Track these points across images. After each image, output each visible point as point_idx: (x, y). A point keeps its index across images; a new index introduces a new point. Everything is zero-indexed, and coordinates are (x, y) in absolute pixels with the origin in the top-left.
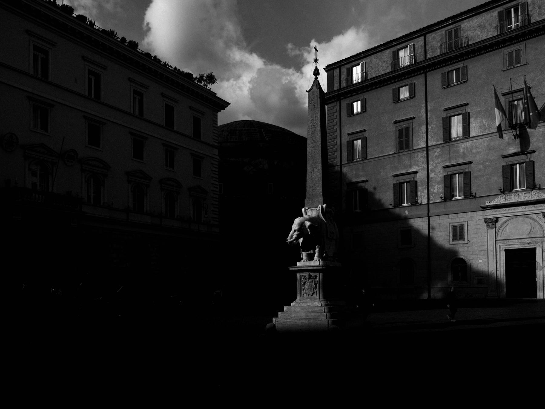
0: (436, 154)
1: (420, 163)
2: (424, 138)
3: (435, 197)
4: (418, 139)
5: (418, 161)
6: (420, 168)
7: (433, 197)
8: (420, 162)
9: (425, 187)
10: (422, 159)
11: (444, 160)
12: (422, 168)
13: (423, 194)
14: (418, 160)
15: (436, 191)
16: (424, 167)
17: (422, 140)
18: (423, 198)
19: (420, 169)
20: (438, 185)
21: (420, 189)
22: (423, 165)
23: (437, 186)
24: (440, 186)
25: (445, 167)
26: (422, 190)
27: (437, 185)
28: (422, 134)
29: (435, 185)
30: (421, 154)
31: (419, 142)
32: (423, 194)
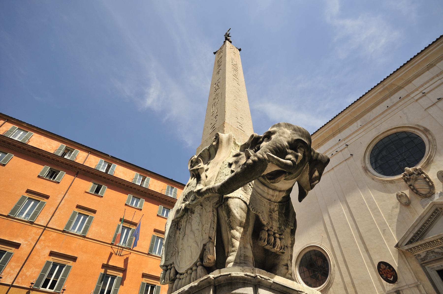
0: (50, 237)
2: (48, 218)
3: (23, 280)
5: (28, 235)
6: (27, 242)
7: (22, 279)
8: (31, 237)
9: (19, 264)
10: (34, 235)
11: (55, 245)
13: (12, 272)
14: (29, 234)
15: (28, 274)
16: (31, 244)
17: (45, 218)
18: (9, 276)
19: (25, 244)
20: (34, 268)
21: (12, 265)
24: (37, 270)
25: (52, 254)
26: (13, 267)
27: (33, 268)
28: (48, 214)
29: (32, 267)
30: (36, 230)
32: (12, 272)
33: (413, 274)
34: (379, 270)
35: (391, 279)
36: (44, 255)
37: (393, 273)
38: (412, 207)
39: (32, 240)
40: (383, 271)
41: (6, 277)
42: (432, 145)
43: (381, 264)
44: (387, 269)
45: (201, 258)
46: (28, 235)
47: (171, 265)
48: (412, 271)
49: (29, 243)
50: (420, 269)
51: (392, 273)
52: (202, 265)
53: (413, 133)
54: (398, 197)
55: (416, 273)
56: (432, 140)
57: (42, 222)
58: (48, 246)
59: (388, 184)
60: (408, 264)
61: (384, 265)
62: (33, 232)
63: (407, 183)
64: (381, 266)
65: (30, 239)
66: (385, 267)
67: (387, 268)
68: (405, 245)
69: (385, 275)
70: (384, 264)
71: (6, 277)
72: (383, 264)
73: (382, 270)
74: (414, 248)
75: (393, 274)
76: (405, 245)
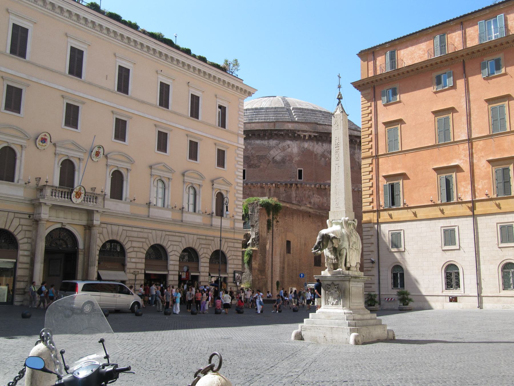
0: (479, 147)
1: (462, 157)
4: (459, 130)
5: (460, 154)
6: (462, 161)
8: (462, 155)
10: (463, 152)
12: (464, 161)
13: (466, 190)
14: (460, 153)
16: (466, 160)
18: (466, 194)
19: (462, 163)
21: (463, 184)
22: (465, 159)
23: (482, 182)
26: (465, 185)
29: (479, 181)
31: (460, 133)
32: (466, 190)
36: (484, 166)
39: (465, 156)
41: (465, 195)
46: (460, 154)
49: (464, 161)
57: (463, 136)
58: (483, 157)
62: (461, 150)
65: (462, 157)
71: (465, 195)
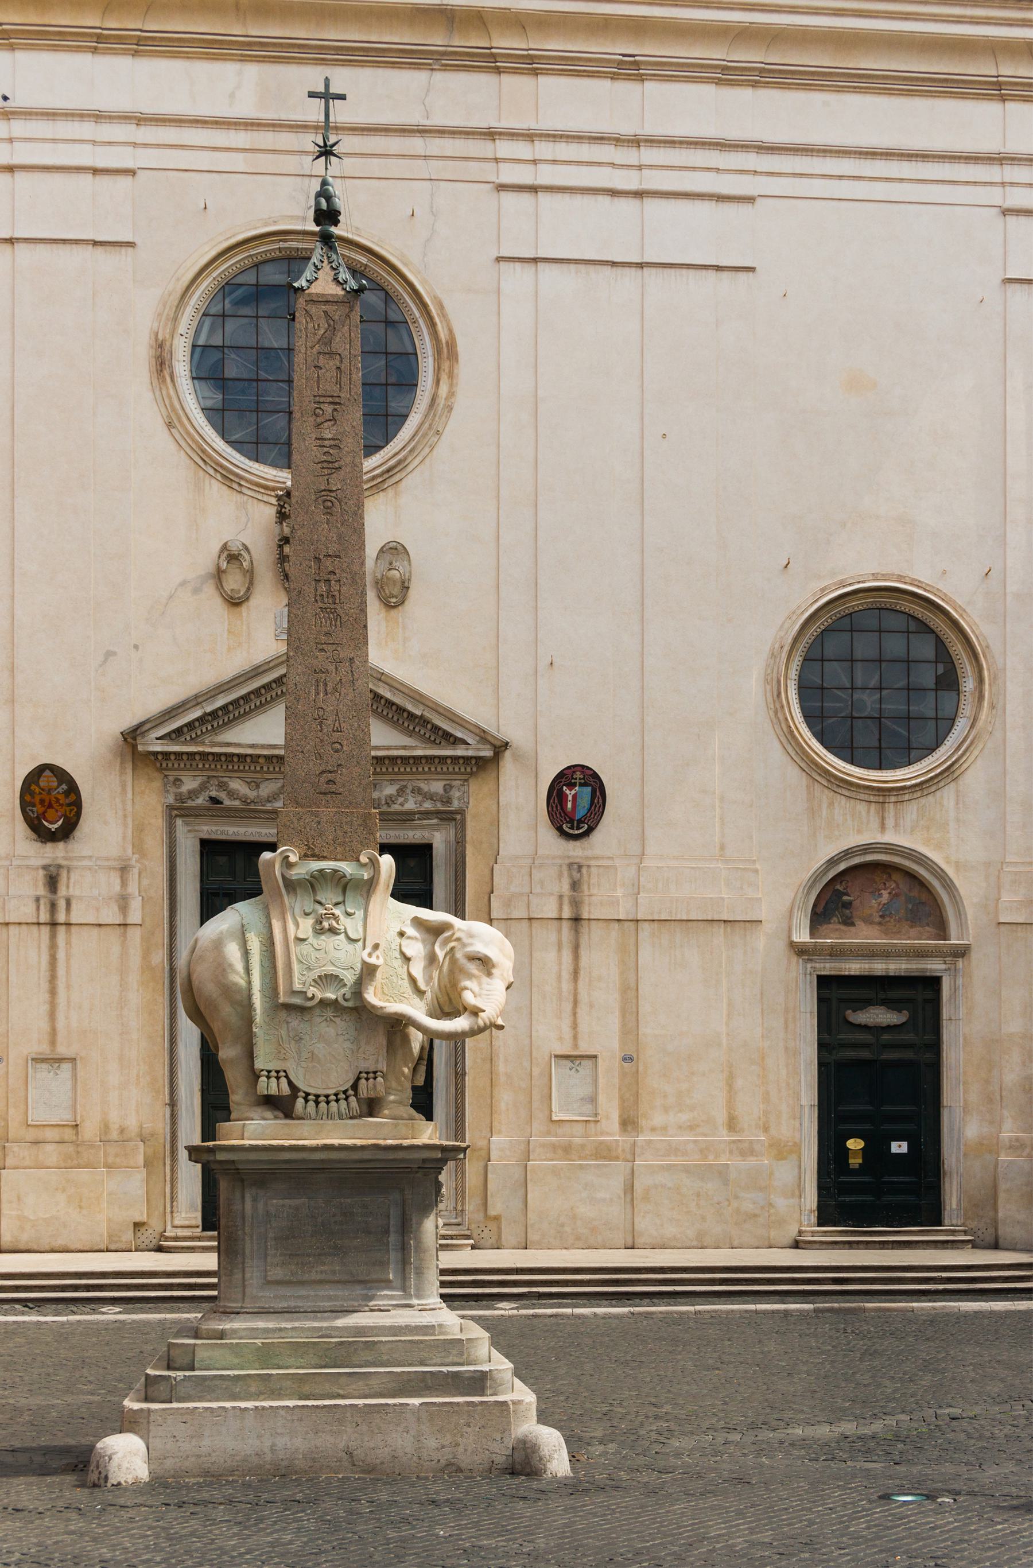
33: (130, 831)
34: (30, 786)
35: (50, 826)
37: (71, 811)
38: (244, 614)
40: (40, 793)
42: (430, 427)
43: (47, 773)
44: (58, 792)
45: (355, 1087)
47: (278, 1072)
48: (130, 821)
50: (158, 822)
51: (68, 809)
52: (356, 1095)
53: (407, 322)
54: (223, 557)
55: (139, 829)
56: (443, 402)
59: (213, 481)
60: (130, 795)
61: (55, 779)
63: (281, 523)
64: (41, 779)
66: (56, 784)
67: (60, 790)
68: (157, 739)
69: (38, 809)
70: (55, 776)
72: (50, 774)
73: (37, 790)
74: (179, 755)
75: (68, 813)
76: (157, 739)
